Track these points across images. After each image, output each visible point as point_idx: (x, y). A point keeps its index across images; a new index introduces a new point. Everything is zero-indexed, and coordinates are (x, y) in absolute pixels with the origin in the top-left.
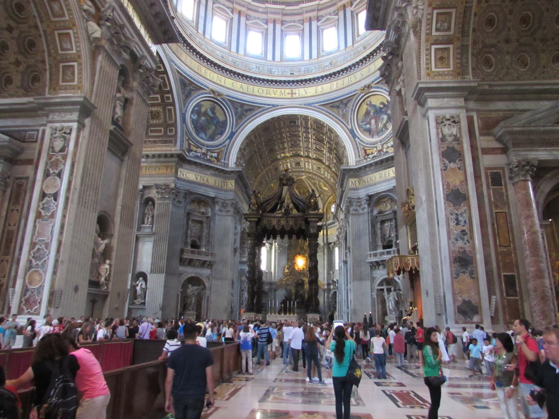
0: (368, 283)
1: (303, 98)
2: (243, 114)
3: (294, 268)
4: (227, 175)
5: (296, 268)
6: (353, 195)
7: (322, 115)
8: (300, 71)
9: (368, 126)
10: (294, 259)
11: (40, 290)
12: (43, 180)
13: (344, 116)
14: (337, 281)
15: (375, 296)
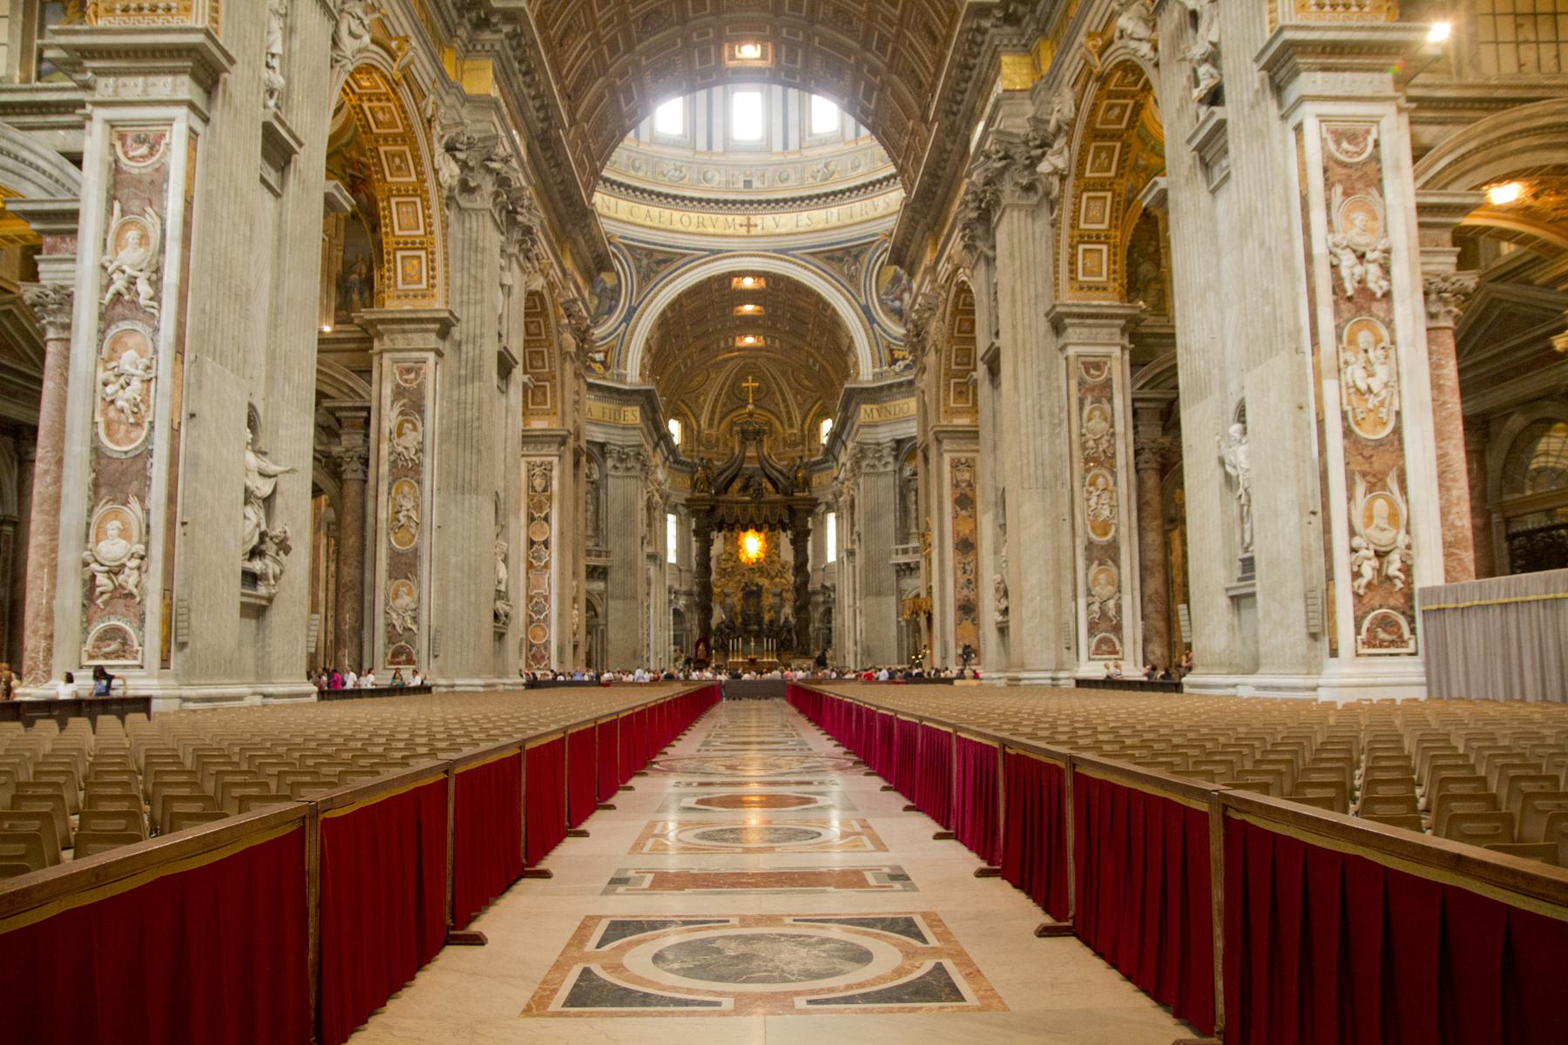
0: (893, 599)
1: (771, 236)
2: (652, 270)
3: (738, 559)
4: (626, 397)
5: (743, 558)
6: (866, 436)
7: (809, 274)
8: (763, 175)
9: (897, 304)
10: (737, 539)
11: (546, 645)
12: (528, 526)
13: (852, 278)
14: (834, 586)
15: (903, 624)
